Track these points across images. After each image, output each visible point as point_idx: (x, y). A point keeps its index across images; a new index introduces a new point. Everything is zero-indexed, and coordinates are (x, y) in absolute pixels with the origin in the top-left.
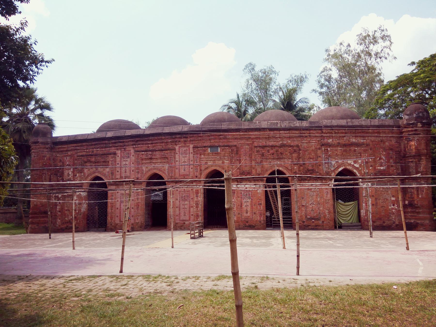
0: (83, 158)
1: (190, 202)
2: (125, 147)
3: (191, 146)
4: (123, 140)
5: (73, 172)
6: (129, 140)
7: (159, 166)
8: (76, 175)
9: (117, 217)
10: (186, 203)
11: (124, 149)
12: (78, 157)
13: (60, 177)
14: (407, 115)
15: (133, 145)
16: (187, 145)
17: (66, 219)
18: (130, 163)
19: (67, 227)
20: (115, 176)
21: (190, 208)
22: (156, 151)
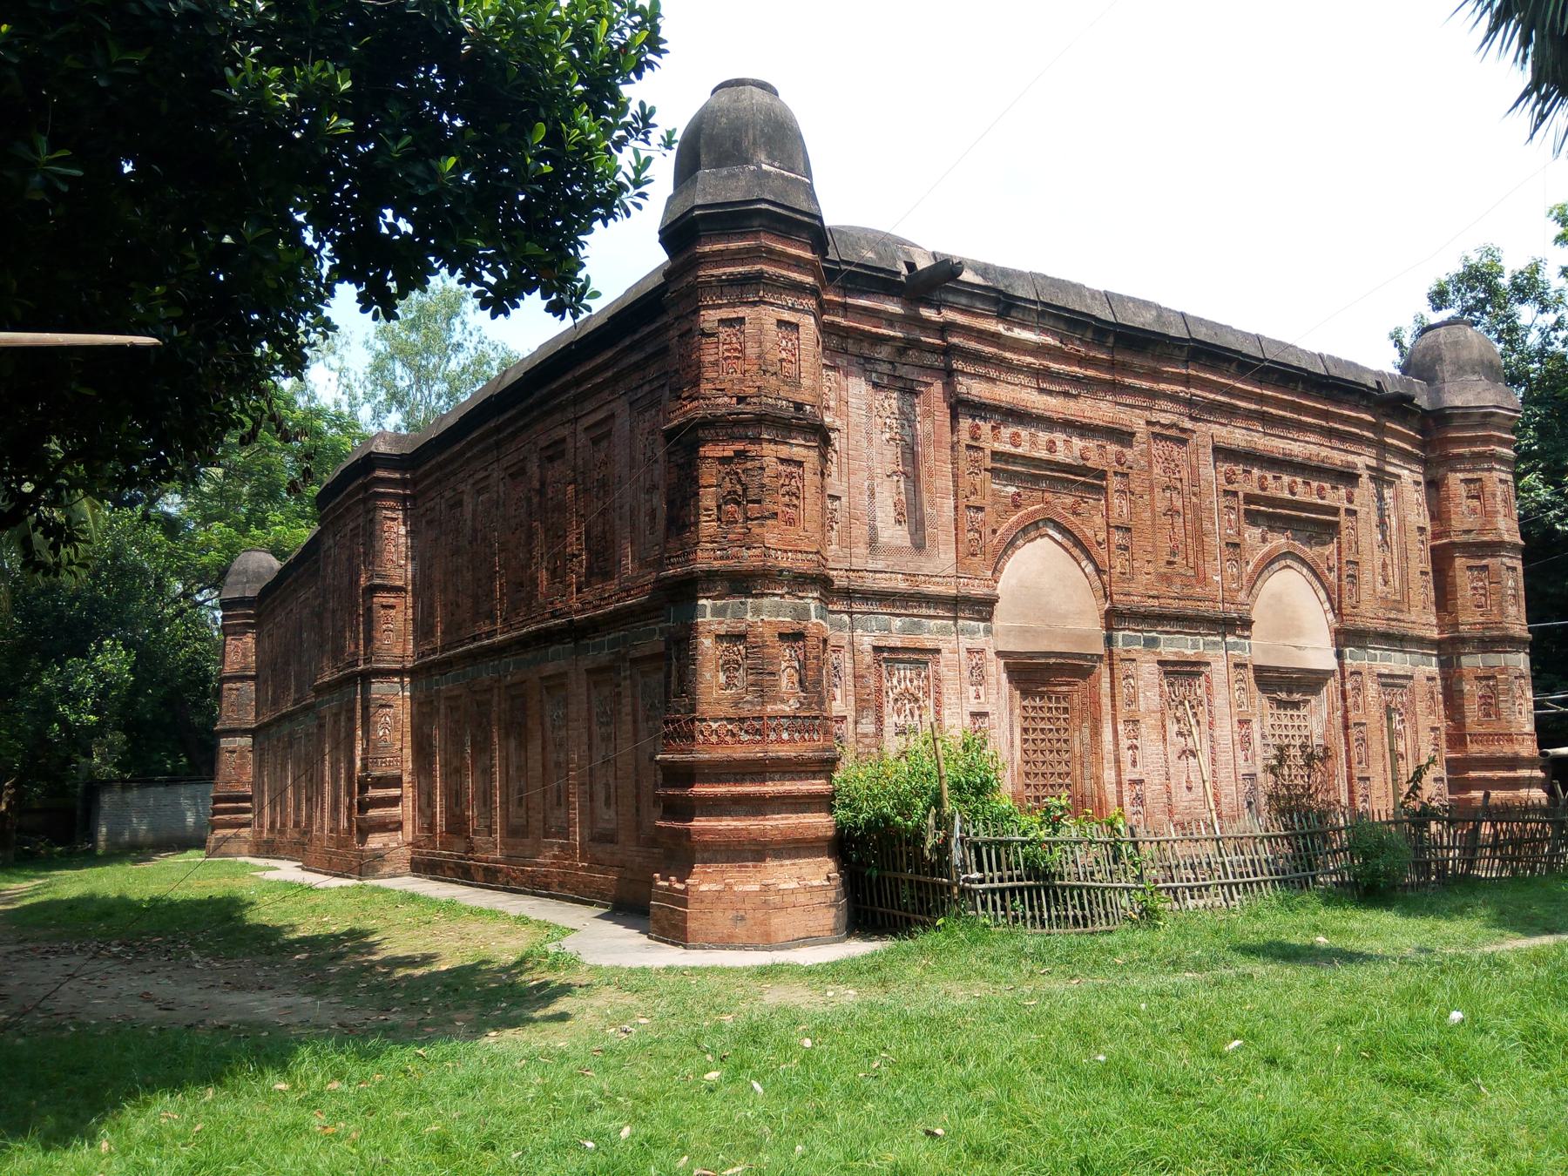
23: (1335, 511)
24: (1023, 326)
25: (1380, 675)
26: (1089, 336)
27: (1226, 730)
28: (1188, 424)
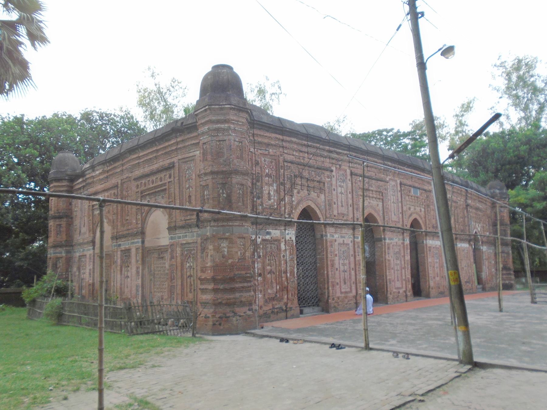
0: (293, 166)
1: (401, 261)
2: (340, 163)
3: (398, 182)
4: (340, 151)
5: (278, 191)
6: (345, 152)
8: (283, 199)
9: (338, 284)
10: (398, 262)
11: (340, 165)
12: (286, 164)
13: (259, 198)
14: (498, 189)
15: (349, 162)
16: (396, 179)
17: (269, 291)
18: (347, 191)
19: (274, 308)
20: (333, 211)
21: (401, 270)
22: (373, 179)
23: (165, 184)
24: (97, 170)
25: (182, 244)
26: (108, 164)
27: (134, 270)
28: (130, 175)
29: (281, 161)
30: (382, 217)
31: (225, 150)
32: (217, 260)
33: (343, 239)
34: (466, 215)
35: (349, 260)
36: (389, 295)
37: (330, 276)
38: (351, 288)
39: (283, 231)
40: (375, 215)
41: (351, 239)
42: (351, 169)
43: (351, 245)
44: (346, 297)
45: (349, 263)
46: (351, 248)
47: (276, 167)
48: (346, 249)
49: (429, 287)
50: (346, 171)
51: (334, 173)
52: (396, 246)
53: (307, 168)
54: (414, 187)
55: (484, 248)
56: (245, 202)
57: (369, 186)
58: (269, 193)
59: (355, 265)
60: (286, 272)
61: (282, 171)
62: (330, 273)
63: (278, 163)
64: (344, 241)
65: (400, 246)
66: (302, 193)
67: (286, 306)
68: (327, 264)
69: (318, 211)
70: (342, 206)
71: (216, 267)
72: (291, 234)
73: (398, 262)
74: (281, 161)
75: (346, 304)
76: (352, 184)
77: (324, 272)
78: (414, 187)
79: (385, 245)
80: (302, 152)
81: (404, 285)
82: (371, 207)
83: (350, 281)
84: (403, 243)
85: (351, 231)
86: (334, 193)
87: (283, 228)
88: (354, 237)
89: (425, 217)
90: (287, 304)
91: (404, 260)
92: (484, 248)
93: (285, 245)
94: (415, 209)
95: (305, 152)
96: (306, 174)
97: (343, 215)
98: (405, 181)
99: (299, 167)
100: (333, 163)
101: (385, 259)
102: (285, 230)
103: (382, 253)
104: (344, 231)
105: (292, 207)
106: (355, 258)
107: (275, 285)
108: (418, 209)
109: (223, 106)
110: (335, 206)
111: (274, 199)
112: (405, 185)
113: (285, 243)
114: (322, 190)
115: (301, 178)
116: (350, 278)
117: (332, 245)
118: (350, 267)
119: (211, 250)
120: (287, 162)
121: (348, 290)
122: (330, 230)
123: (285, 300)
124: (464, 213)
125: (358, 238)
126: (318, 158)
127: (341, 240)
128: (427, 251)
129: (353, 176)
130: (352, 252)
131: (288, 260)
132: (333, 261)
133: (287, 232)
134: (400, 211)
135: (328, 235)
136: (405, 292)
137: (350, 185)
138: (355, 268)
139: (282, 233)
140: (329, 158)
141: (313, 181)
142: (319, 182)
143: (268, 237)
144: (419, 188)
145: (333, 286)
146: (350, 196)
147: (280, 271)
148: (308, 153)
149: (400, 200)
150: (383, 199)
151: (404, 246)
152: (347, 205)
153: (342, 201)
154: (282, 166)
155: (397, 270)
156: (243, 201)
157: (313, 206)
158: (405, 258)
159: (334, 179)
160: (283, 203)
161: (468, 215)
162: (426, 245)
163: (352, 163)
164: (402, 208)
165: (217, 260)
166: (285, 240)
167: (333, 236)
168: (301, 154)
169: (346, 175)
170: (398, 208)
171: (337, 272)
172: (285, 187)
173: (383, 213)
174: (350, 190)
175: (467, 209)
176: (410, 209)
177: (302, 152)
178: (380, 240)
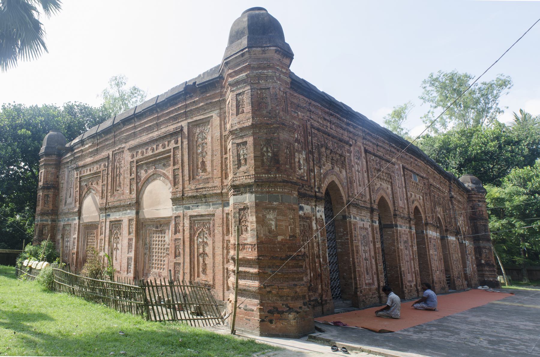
0: (319, 134)
1: (409, 252)
3: (401, 166)
5: (307, 160)
6: (360, 127)
7: (385, 185)
11: (356, 141)
12: (313, 130)
15: (364, 138)
18: (362, 170)
20: (354, 190)
22: (383, 160)
29: (309, 127)
30: (392, 201)
31: (269, 100)
32: (262, 235)
33: (362, 222)
34: (451, 207)
35: (369, 247)
36: (405, 289)
37: (356, 264)
38: (373, 279)
39: (314, 207)
40: (387, 198)
41: (369, 223)
42: (365, 146)
43: (370, 229)
44: (370, 290)
45: (370, 250)
46: (370, 233)
47: (304, 133)
48: (365, 233)
49: (433, 281)
50: (360, 148)
51: (352, 149)
52: (405, 234)
53: (330, 138)
54: (414, 173)
55: (467, 243)
56: (293, 165)
57: (380, 166)
58: (299, 162)
59: (375, 253)
60: (318, 257)
61: (310, 138)
62: (356, 260)
63: (305, 129)
64: (363, 224)
65: (407, 234)
66: (326, 166)
67: (321, 299)
68: (353, 250)
69: (341, 189)
70: (360, 186)
71: (262, 245)
72: (320, 212)
73: (407, 252)
74: (309, 127)
75: (371, 298)
76: (367, 162)
77: (350, 258)
78: (414, 173)
79: (397, 232)
80: (325, 119)
81: (414, 278)
82: (383, 189)
83: (372, 271)
84: (410, 232)
85: (369, 214)
86: (353, 169)
87: (314, 204)
88: (372, 221)
89: (424, 206)
90: (322, 295)
91: (413, 251)
92: (467, 243)
93: (316, 224)
94: (415, 196)
95: (328, 121)
96: (330, 145)
97: (362, 195)
98: (407, 166)
99: (326, 136)
100: (350, 138)
101: (398, 248)
102: (316, 206)
103: (394, 240)
104: (364, 213)
105: (320, 180)
106: (374, 245)
107: (309, 271)
108: (418, 196)
109: (266, 48)
110: (355, 184)
111: (304, 169)
112: (408, 169)
113: (317, 221)
114: (343, 165)
115: (327, 148)
116: (372, 267)
117: (355, 228)
118: (370, 256)
119: (252, 223)
120: (314, 128)
121: (371, 281)
122: (353, 211)
123: (320, 291)
124: (449, 205)
125: (376, 223)
126: (338, 130)
127: (360, 224)
128: (428, 243)
129: (368, 154)
130: (371, 239)
131: (320, 241)
132: (357, 247)
133: (317, 208)
134: (405, 197)
135: (352, 216)
136: (416, 285)
137: (365, 163)
138: (376, 257)
139: (312, 209)
140: (348, 131)
141: (336, 153)
142: (341, 156)
143: (301, 213)
144: (418, 175)
145: (360, 277)
146: (366, 175)
147: (313, 254)
148: (330, 122)
149: (404, 185)
150: (391, 183)
151: (411, 234)
152: (364, 185)
153: (359, 180)
154: (309, 133)
155: (408, 262)
156: (291, 163)
157: (337, 182)
158: (413, 248)
159: (352, 154)
160: (313, 174)
161: (453, 207)
162: (427, 235)
163: (366, 139)
164: (407, 194)
165: (262, 235)
166: (316, 218)
167: (356, 218)
168: (325, 123)
169: (361, 152)
170: (403, 193)
171: (361, 259)
172: (313, 156)
173: (393, 198)
174: (365, 169)
175: (451, 201)
176: (411, 195)
177: (325, 119)
178: (391, 226)
